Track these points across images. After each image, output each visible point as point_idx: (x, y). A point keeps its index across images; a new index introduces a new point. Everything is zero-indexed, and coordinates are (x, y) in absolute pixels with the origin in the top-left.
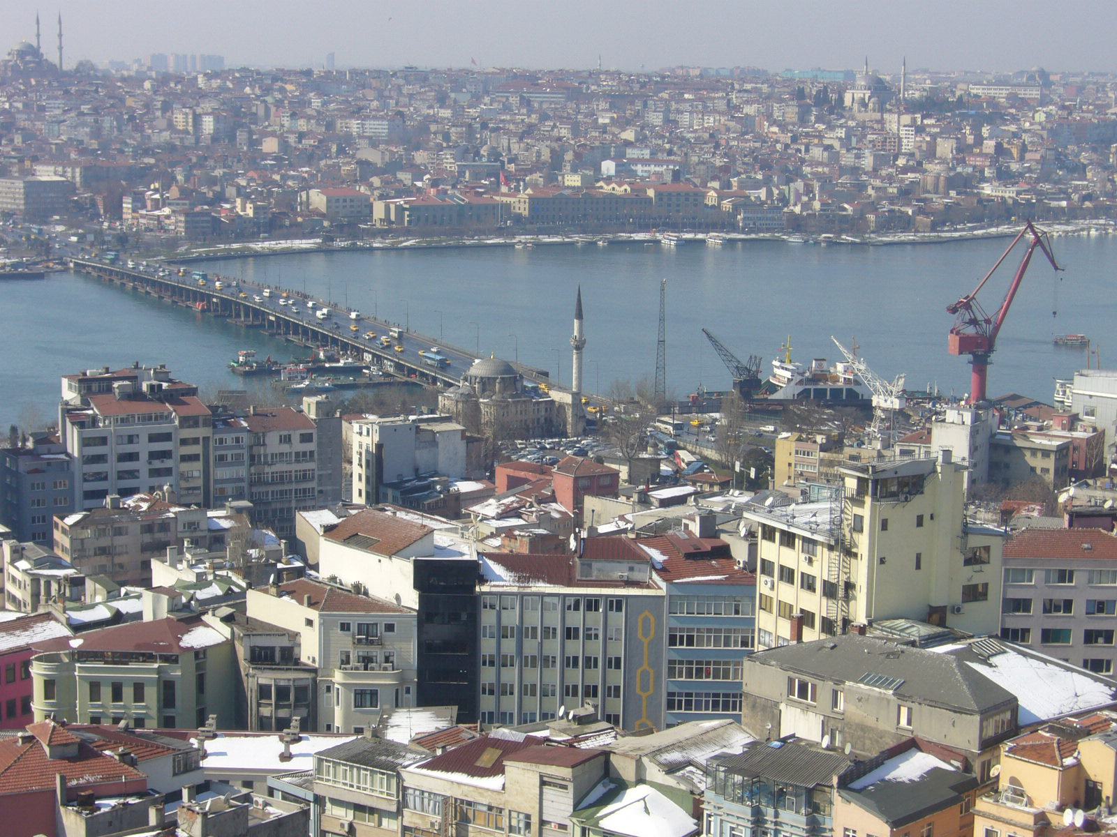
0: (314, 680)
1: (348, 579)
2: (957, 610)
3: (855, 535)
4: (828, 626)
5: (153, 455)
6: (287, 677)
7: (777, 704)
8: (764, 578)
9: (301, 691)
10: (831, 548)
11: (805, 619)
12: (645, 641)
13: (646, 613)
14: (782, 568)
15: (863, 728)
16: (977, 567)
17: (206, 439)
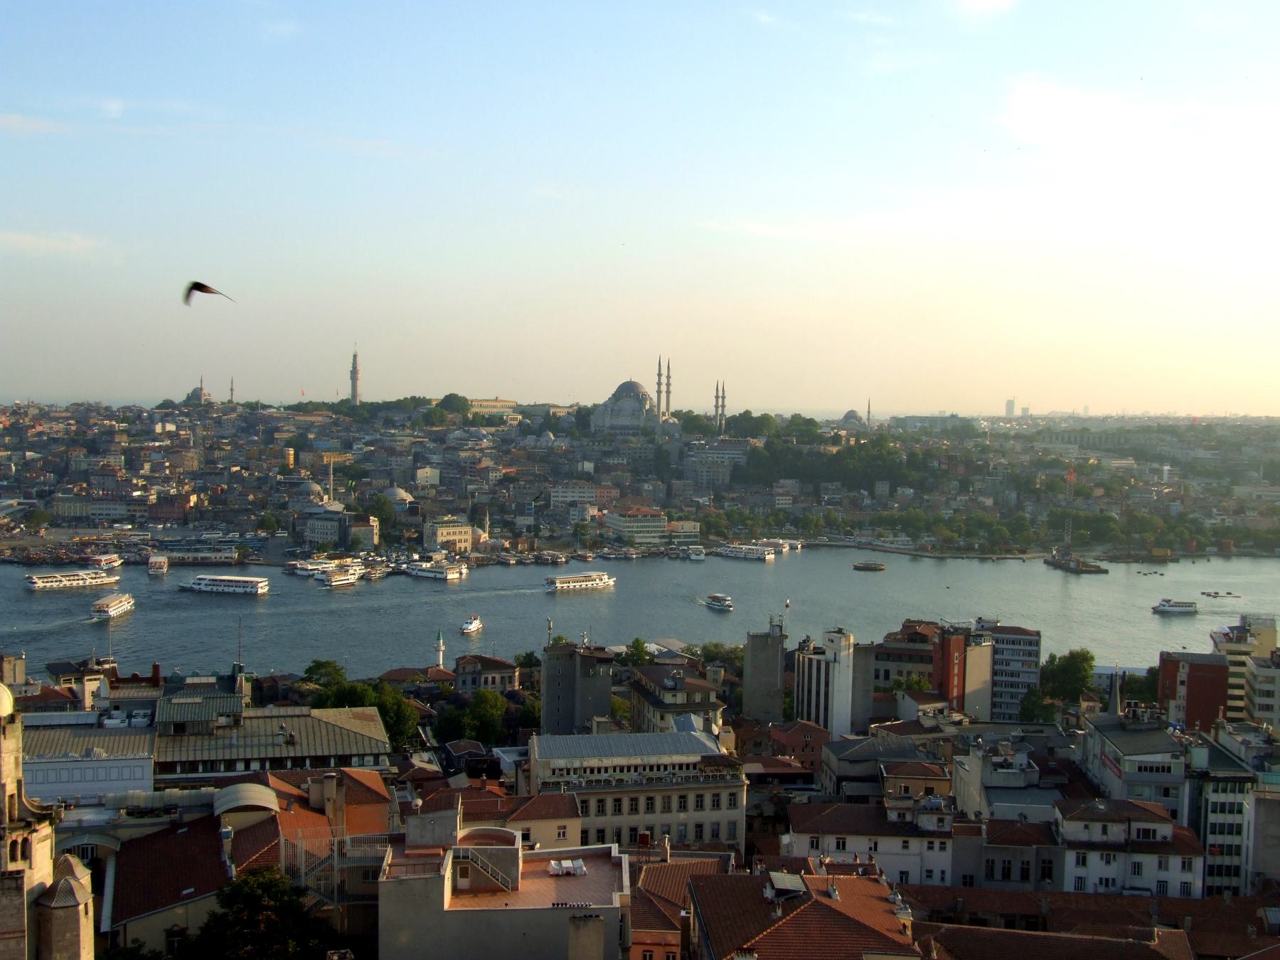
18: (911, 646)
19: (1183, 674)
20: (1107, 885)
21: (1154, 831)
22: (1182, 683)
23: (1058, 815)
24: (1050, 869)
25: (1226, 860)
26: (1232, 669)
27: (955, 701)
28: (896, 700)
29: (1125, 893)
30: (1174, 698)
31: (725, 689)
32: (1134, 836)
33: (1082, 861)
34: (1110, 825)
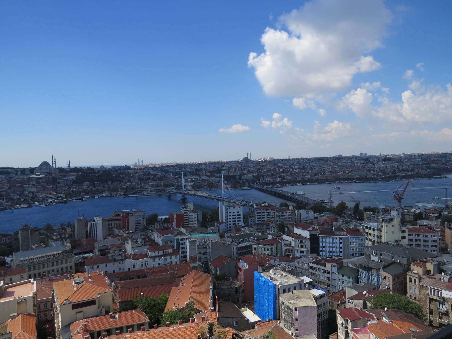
0: (294, 249)
1: (299, 234)
2: (400, 241)
3: (382, 228)
4: (378, 242)
5: (267, 215)
6: (290, 248)
7: (370, 255)
8: (366, 235)
9: (292, 251)
10: (378, 230)
11: (374, 241)
12: (346, 244)
13: (346, 240)
14: (369, 233)
15: (385, 259)
16: (403, 234)
17: (275, 213)
18: (116, 217)
19: (175, 216)
20: (160, 265)
21: (169, 251)
22: (175, 218)
23: (148, 251)
24: (147, 263)
25: (184, 255)
26: (185, 214)
27: (127, 229)
28: (113, 230)
29: (164, 265)
30: (174, 222)
31: (72, 233)
32: (165, 253)
33: (154, 261)
34: (160, 252)
